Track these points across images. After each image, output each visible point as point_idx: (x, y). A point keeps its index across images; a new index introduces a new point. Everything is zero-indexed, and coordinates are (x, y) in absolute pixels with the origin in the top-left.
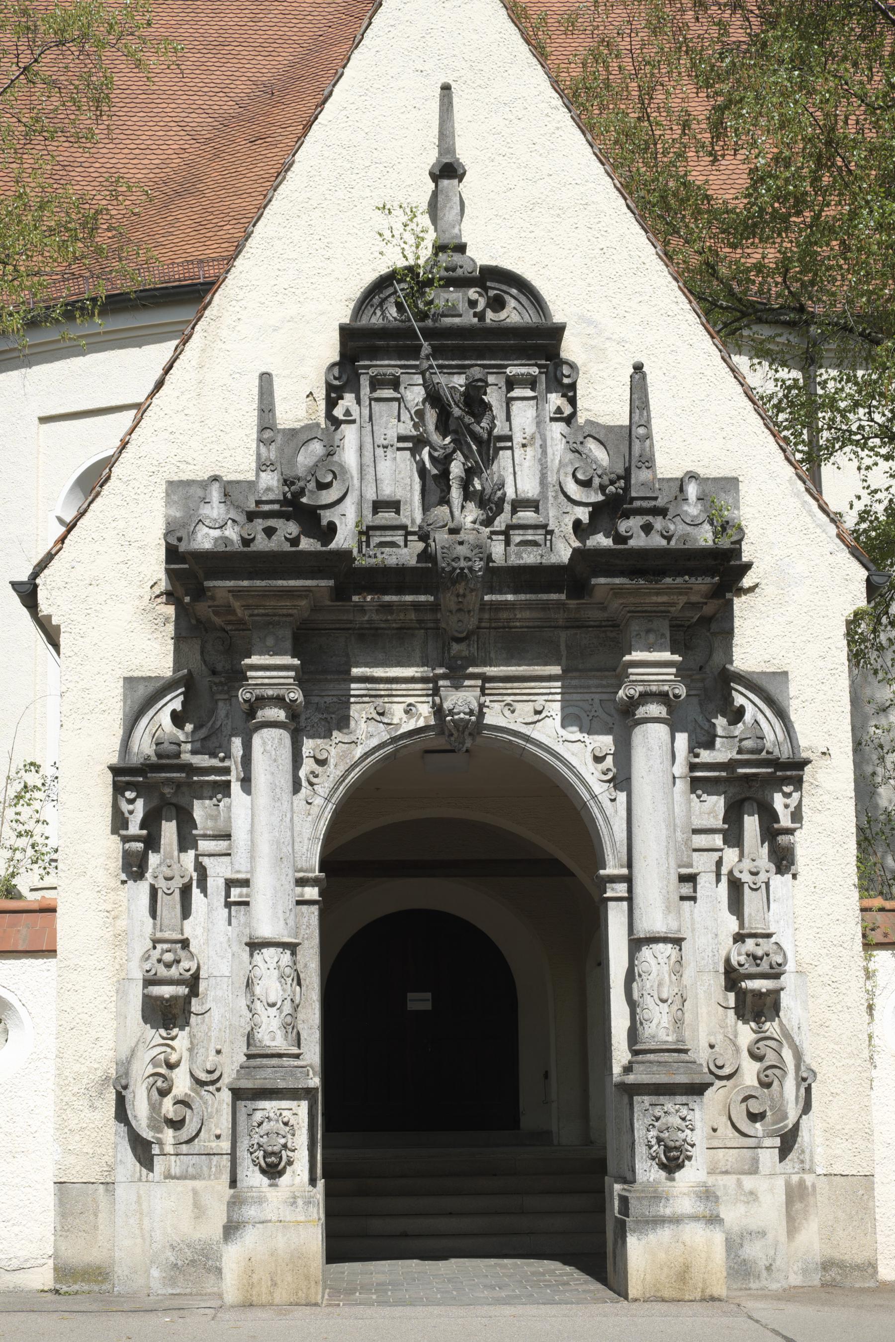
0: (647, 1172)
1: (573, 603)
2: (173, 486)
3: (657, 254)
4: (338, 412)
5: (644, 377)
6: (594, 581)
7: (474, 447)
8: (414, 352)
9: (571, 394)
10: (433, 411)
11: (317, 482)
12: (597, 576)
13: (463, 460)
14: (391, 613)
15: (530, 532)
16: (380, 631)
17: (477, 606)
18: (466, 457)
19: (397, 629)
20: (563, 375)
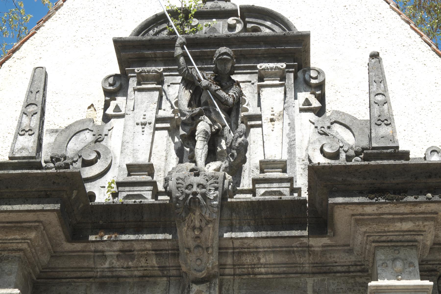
1: (318, 243)
3: (391, 7)
4: (110, 111)
5: (380, 61)
6: (331, 201)
7: (223, 116)
9: (319, 92)
10: (187, 92)
11: (83, 161)
12: (334, 196)
13: (210, 122)
14: (132, 258)
15: (275, 185)
16: (121, 280)
17: (216, 244)
18: (214, 122)
19: (140, 277)
20: (311, 77)
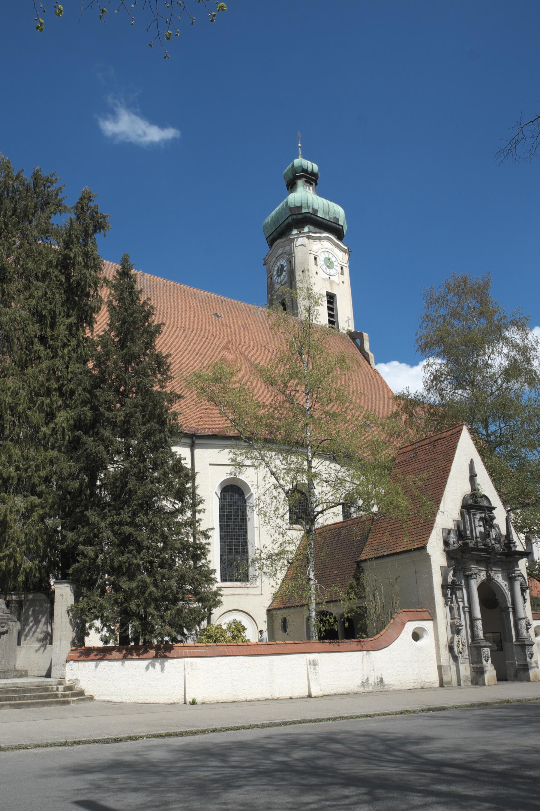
0: (528, 659)
2: (443, 530)
8: (485, 510)
